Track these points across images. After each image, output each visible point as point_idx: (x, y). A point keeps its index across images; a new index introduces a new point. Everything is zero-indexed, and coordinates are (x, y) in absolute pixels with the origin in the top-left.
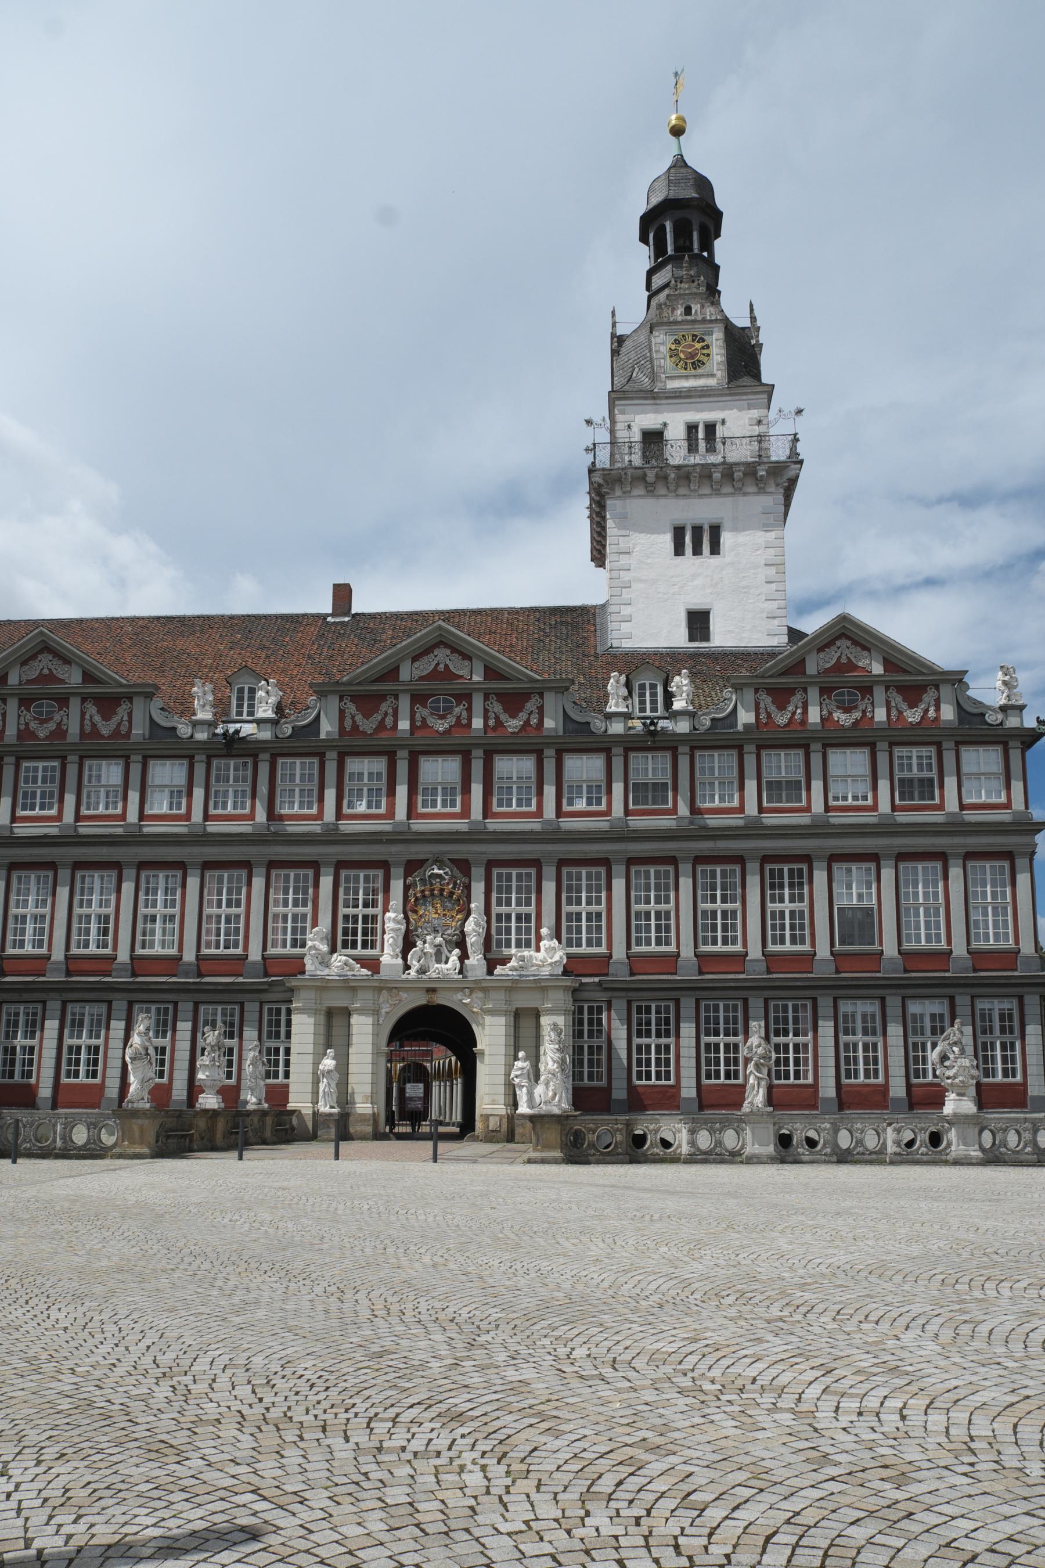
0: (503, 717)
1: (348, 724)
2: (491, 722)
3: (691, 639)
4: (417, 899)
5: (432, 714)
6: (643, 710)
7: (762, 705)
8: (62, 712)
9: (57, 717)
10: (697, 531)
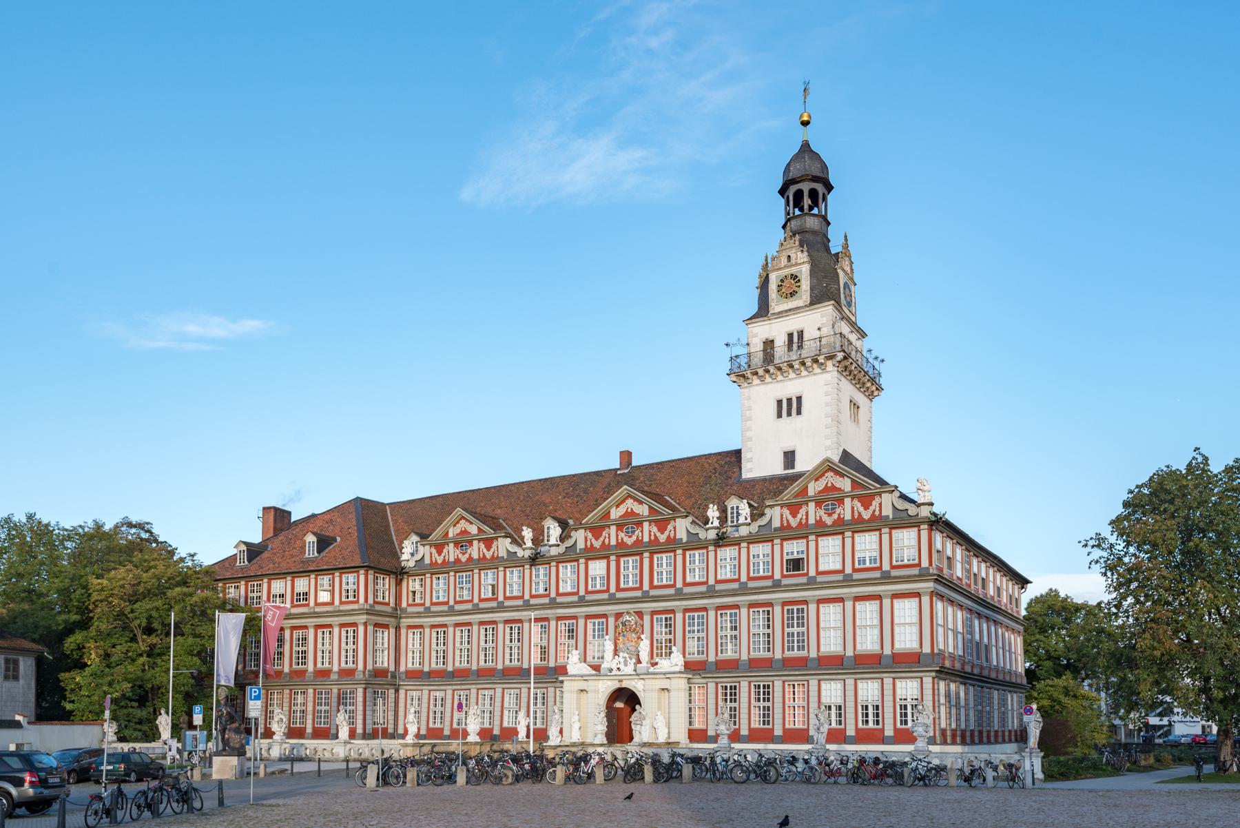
0: (658, 534)
3: (786, 468)
10: (789, 400)
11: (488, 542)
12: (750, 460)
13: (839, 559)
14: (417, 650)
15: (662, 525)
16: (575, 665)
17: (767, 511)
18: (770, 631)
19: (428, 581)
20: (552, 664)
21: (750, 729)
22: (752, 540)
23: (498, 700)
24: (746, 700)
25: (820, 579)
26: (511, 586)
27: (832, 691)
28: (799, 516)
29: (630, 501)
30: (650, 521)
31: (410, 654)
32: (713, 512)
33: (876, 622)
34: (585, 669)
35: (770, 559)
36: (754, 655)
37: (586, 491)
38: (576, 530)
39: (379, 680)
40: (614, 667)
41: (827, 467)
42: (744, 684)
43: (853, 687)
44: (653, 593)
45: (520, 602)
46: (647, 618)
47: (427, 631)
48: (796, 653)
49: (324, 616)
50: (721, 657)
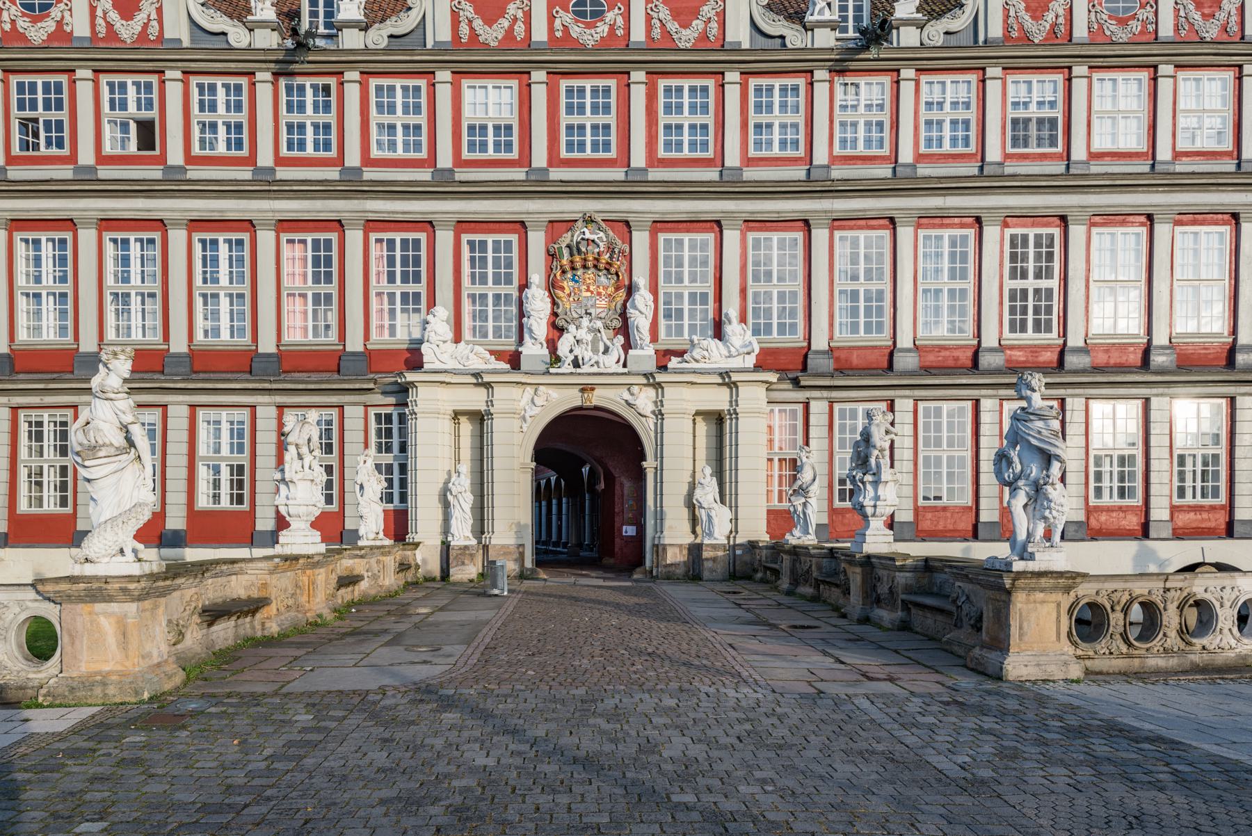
0: (673, 26)
1: (464, 30)
2: (656, 33)
4: (564, 272)
5: (577, 21)
7: (1012, 13)
8: (62, 6)
9: (55, 12)
23: (177, 434)
35: (972, 115)
46: (641, 239)
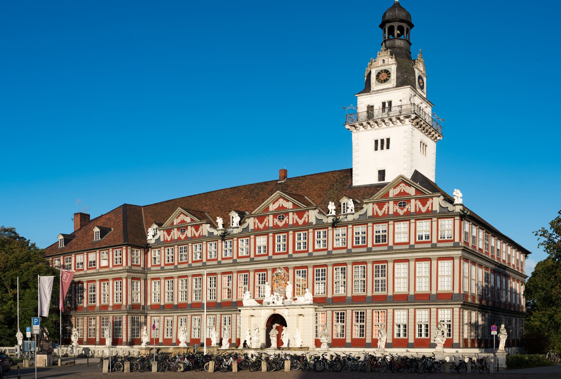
0: (298, 220)
1: (256, 226)
2: (295, 222)
3: (380, 180)
6: (344, 212)
11: (197, 227)
12: (358, 175)
13: (407, 235)
14: (158, 293)
15: (300, 214)
16: (247, 300)
17: (364, 206)
18: (365, 279)
19: (163, 251)
20: (234, 300)
21: (352, 339)
22: (355, 223)
24: (350, 321)
25: (395, 247)
26: (211, 253)
27: (401, 316)
28: (384, 209)
29: (281, 200)
30: (293, 212)
31: (153, 295)
32: (332, 206)
33: (428, 274)
34: (254, 303)
36: (356, 293)
37: (257, 194)
38: (249, 218)
39: (135, 311)
40: (271, 301)
41: (402, 180)
42: (349, 312)
43: (413, 314)
44: (295, 255)
45: (216, 263)
46: (291, 271)
47: (162, 281)
48: (380, 293)
49: (102, 271)
50: (336, 294)
